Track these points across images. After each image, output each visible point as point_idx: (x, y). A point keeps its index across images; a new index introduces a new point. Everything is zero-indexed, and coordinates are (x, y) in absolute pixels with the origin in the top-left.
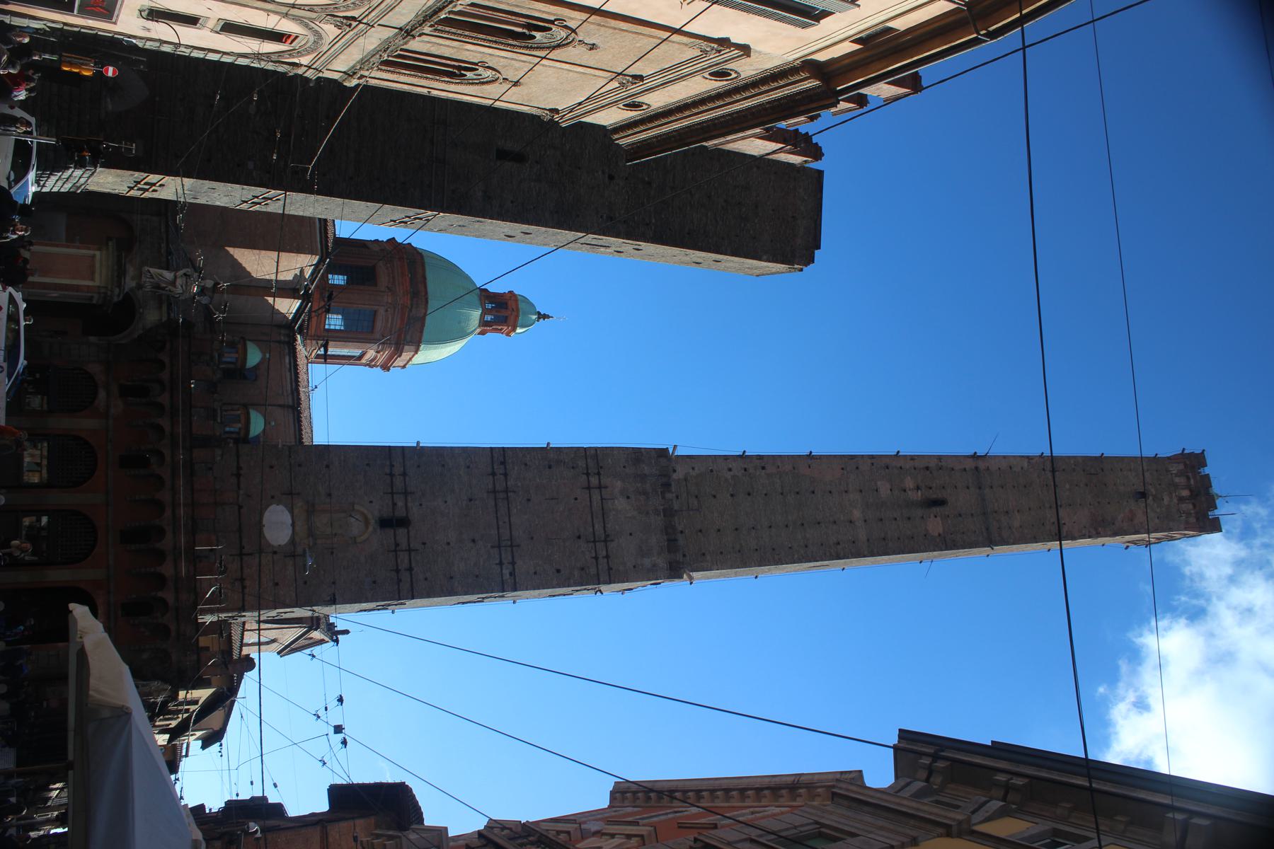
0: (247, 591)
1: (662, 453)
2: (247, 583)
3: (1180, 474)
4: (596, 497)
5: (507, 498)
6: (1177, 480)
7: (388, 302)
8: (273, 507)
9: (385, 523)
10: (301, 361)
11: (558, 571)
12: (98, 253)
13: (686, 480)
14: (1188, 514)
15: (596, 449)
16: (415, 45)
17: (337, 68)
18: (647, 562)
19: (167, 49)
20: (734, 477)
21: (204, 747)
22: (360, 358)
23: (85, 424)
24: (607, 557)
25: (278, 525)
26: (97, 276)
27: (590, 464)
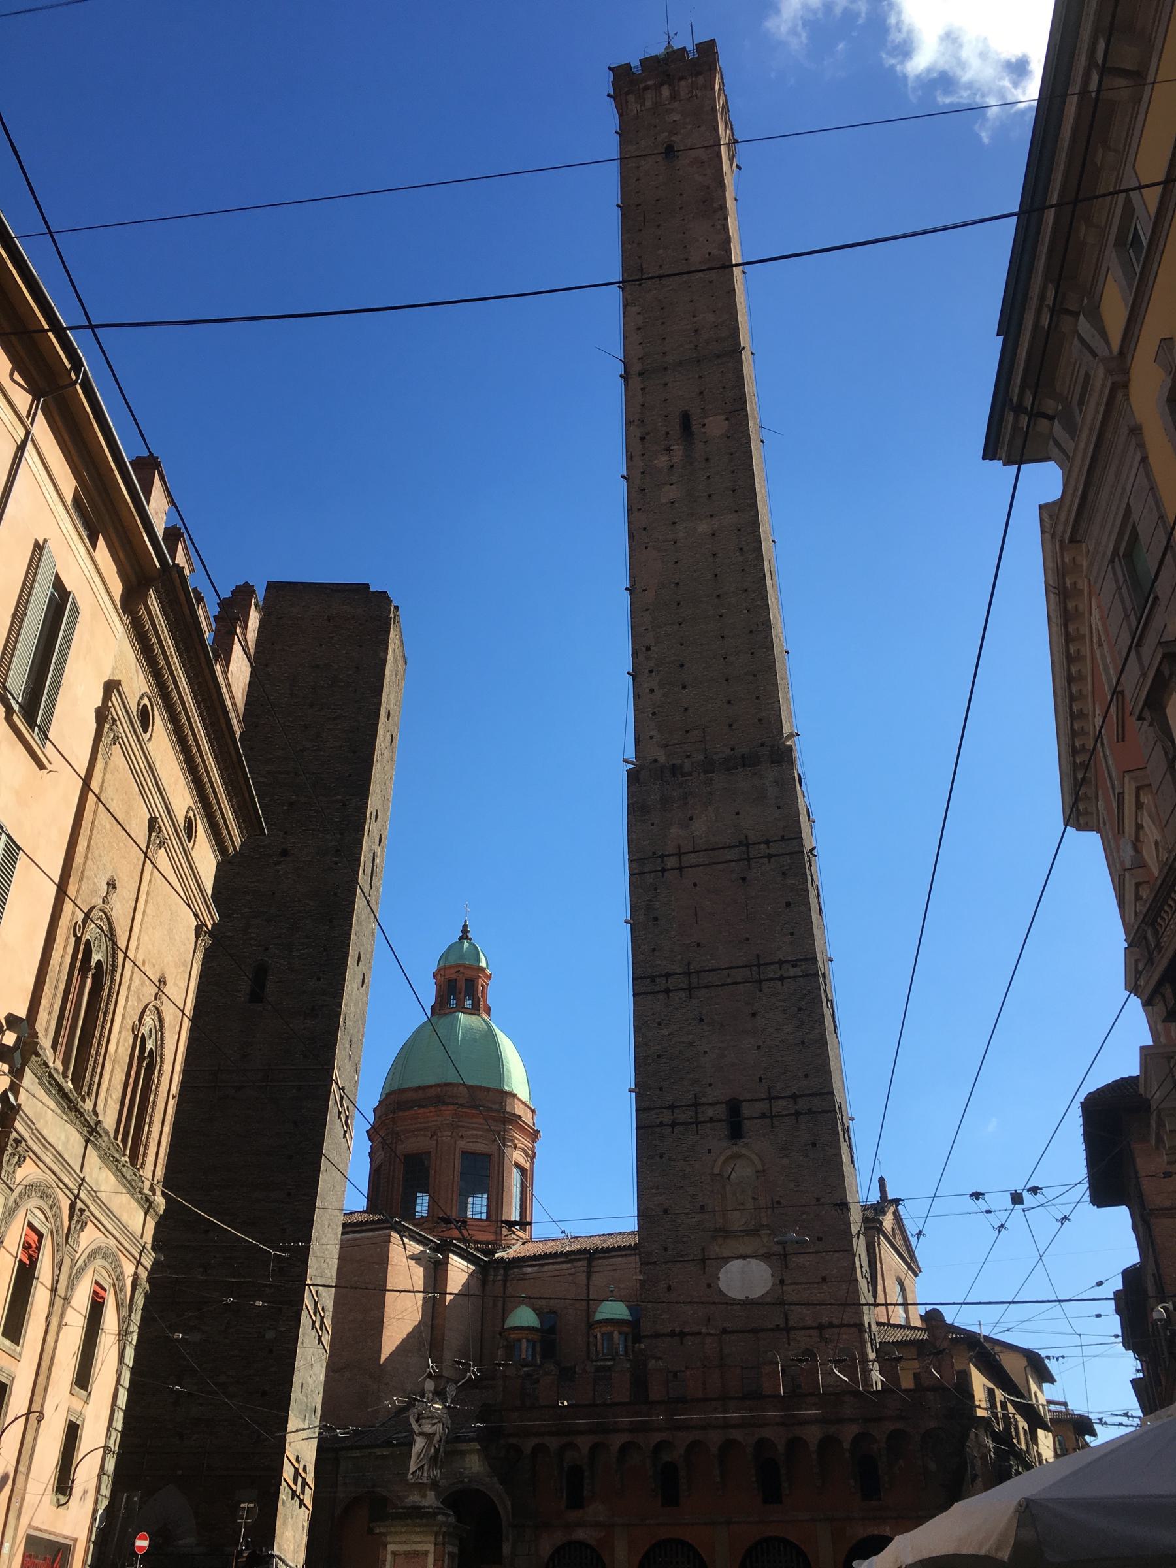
0: (835, 1321)
1: (633, 777)
2: (825, 1320)
4: (691, 859)
5: (698, 972)
6: (649, 104)
7: (449, 1136)
9: (736, 1132)
10: (530, 1250)
11: (788, 904)
12: (390, 1548)
15: (631, 861)
16: (109, 1120)
17: (139, 1224)
19: (110, 1465)
21: (1052, 1380)
22: (523, 1171)
24: (767, 842)
25: (745, 1278)
26: (419, 1548)
27: (650, 869)
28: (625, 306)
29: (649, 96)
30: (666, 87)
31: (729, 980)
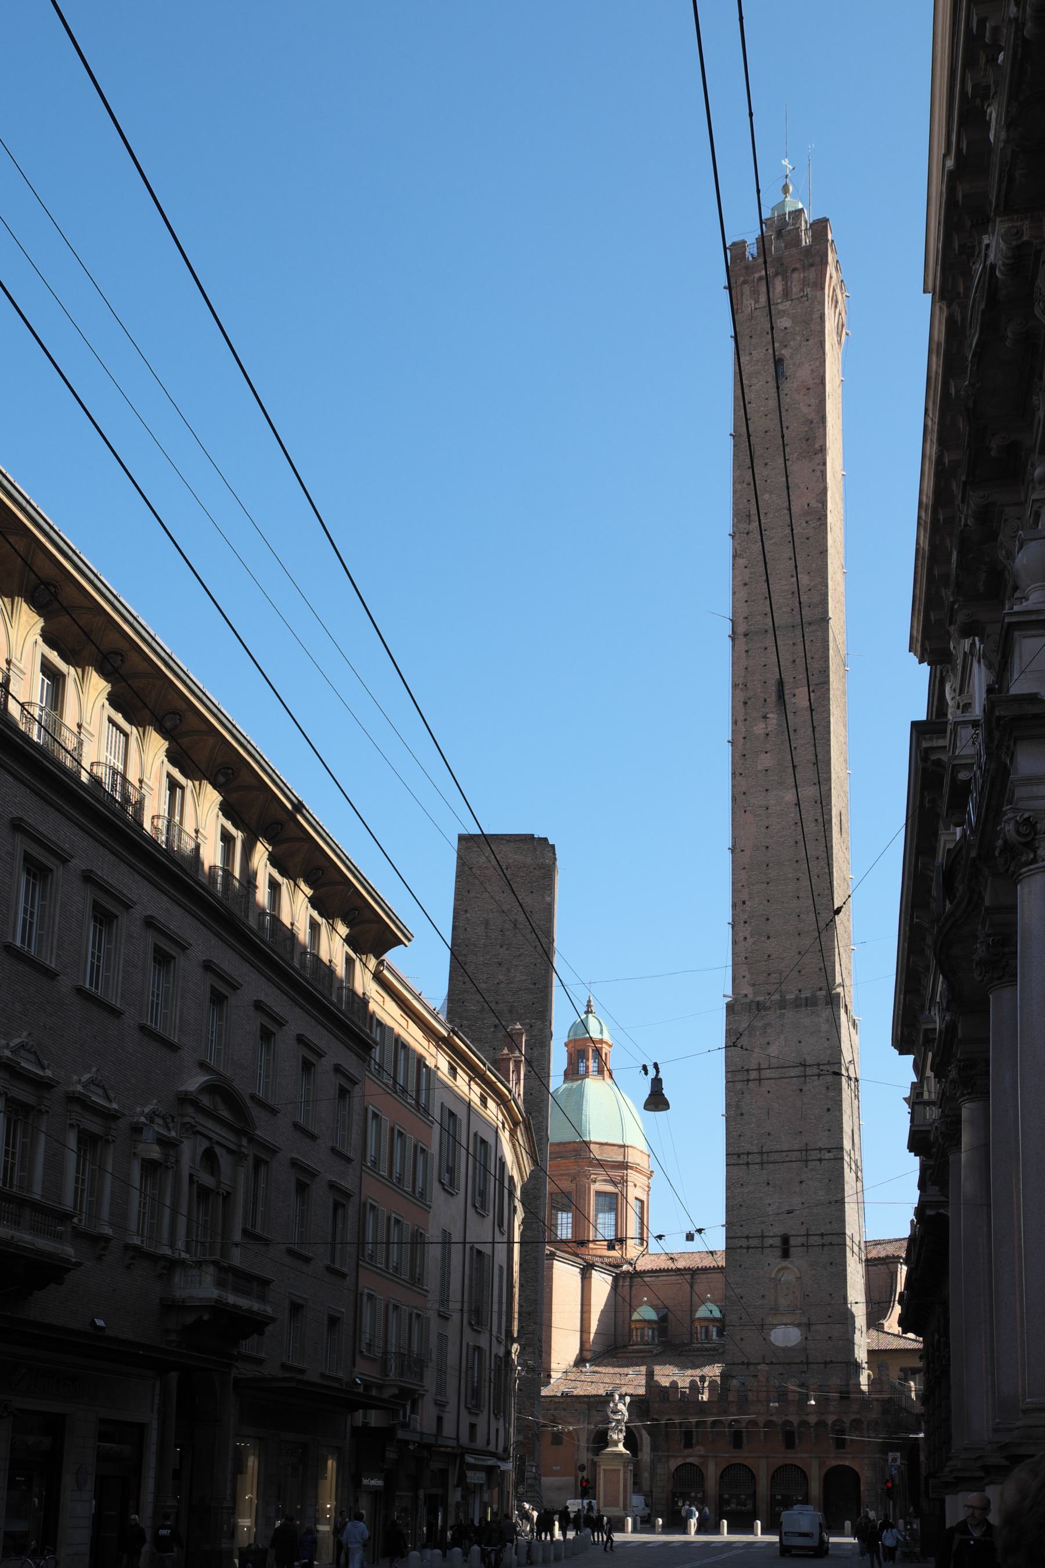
0: (834, 1360)
1: (730, 1008)
2: (828, 1359)
3: (755, 293)
4: (766, 1074)
8: (772, 1339)
9: (786, 1254)
13: (754, 985)
15: (727, 1072)
18: (824, 1027)
20: (752, 936)
25: (785, 1336)
28: (734, 557)
30: (779, 278)
31: (787, 1159)
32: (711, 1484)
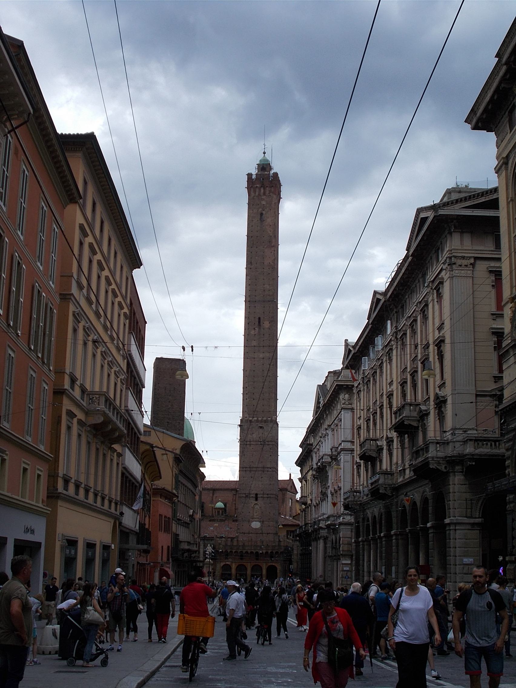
3: (255, 192)
6: (257, 193)
9: (256, 500)
14: (270, 191)
23: (234, 567)
27: (244, 443)
29: (257, 190)
32: (233, 571)
